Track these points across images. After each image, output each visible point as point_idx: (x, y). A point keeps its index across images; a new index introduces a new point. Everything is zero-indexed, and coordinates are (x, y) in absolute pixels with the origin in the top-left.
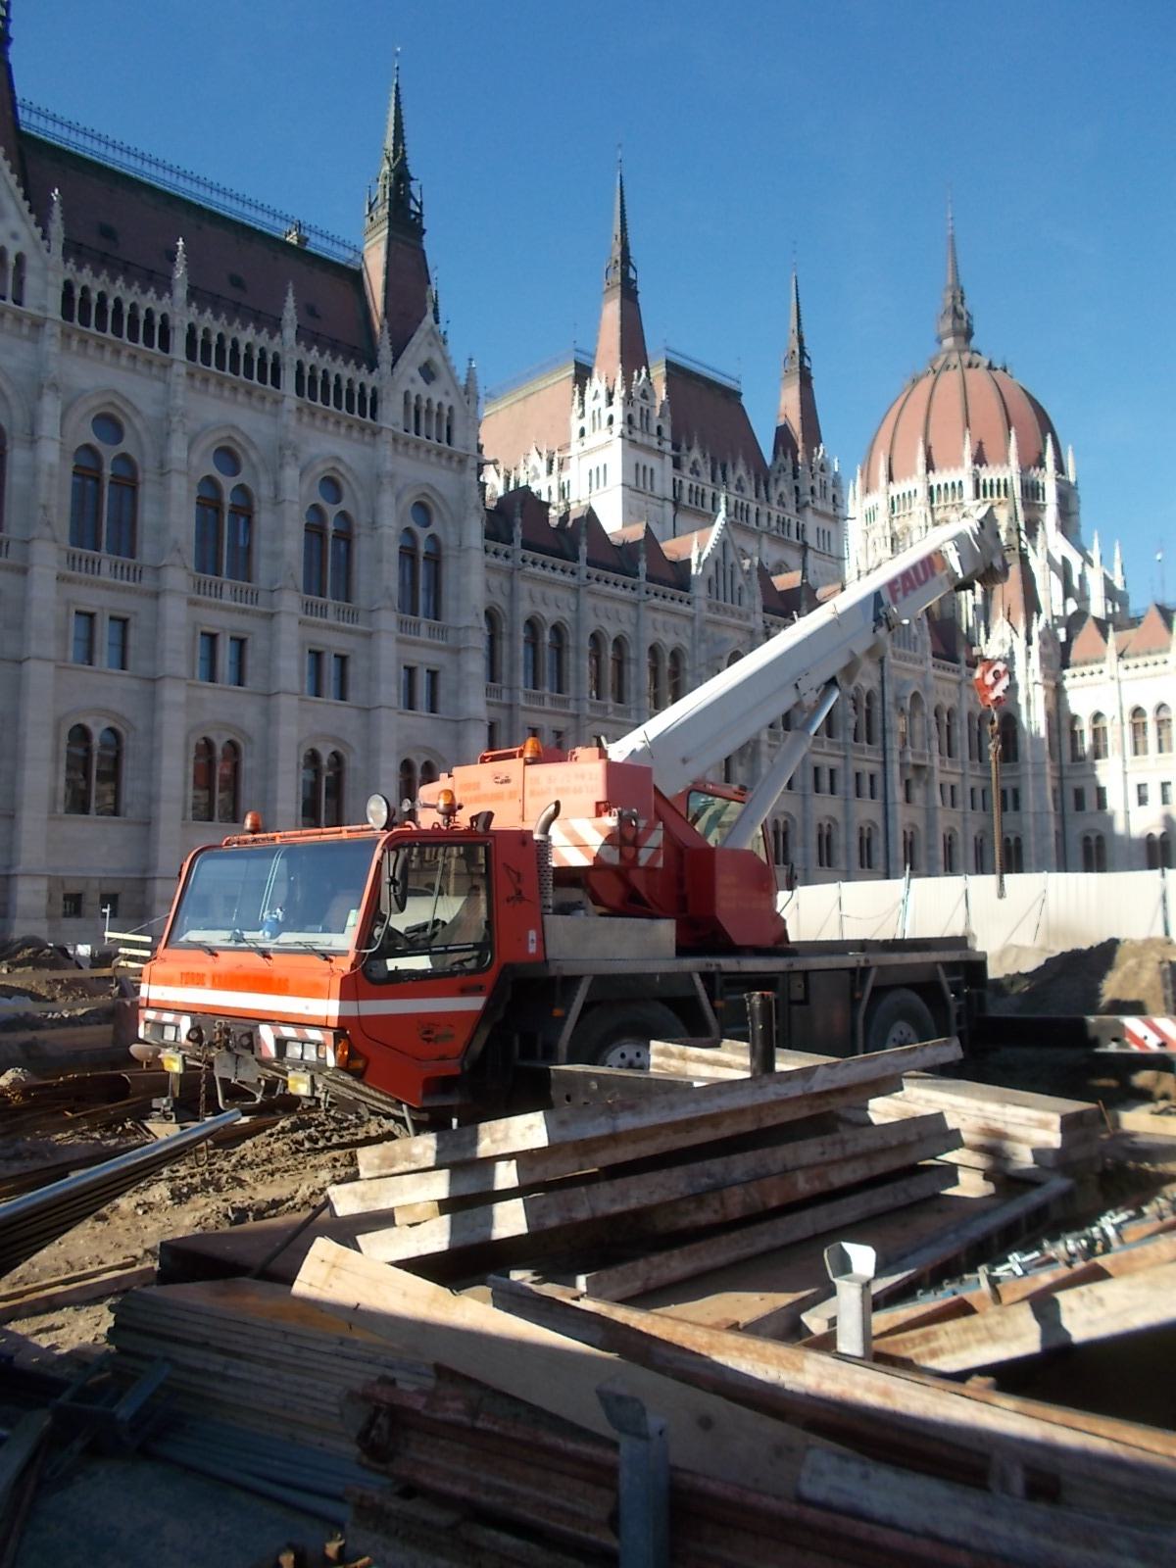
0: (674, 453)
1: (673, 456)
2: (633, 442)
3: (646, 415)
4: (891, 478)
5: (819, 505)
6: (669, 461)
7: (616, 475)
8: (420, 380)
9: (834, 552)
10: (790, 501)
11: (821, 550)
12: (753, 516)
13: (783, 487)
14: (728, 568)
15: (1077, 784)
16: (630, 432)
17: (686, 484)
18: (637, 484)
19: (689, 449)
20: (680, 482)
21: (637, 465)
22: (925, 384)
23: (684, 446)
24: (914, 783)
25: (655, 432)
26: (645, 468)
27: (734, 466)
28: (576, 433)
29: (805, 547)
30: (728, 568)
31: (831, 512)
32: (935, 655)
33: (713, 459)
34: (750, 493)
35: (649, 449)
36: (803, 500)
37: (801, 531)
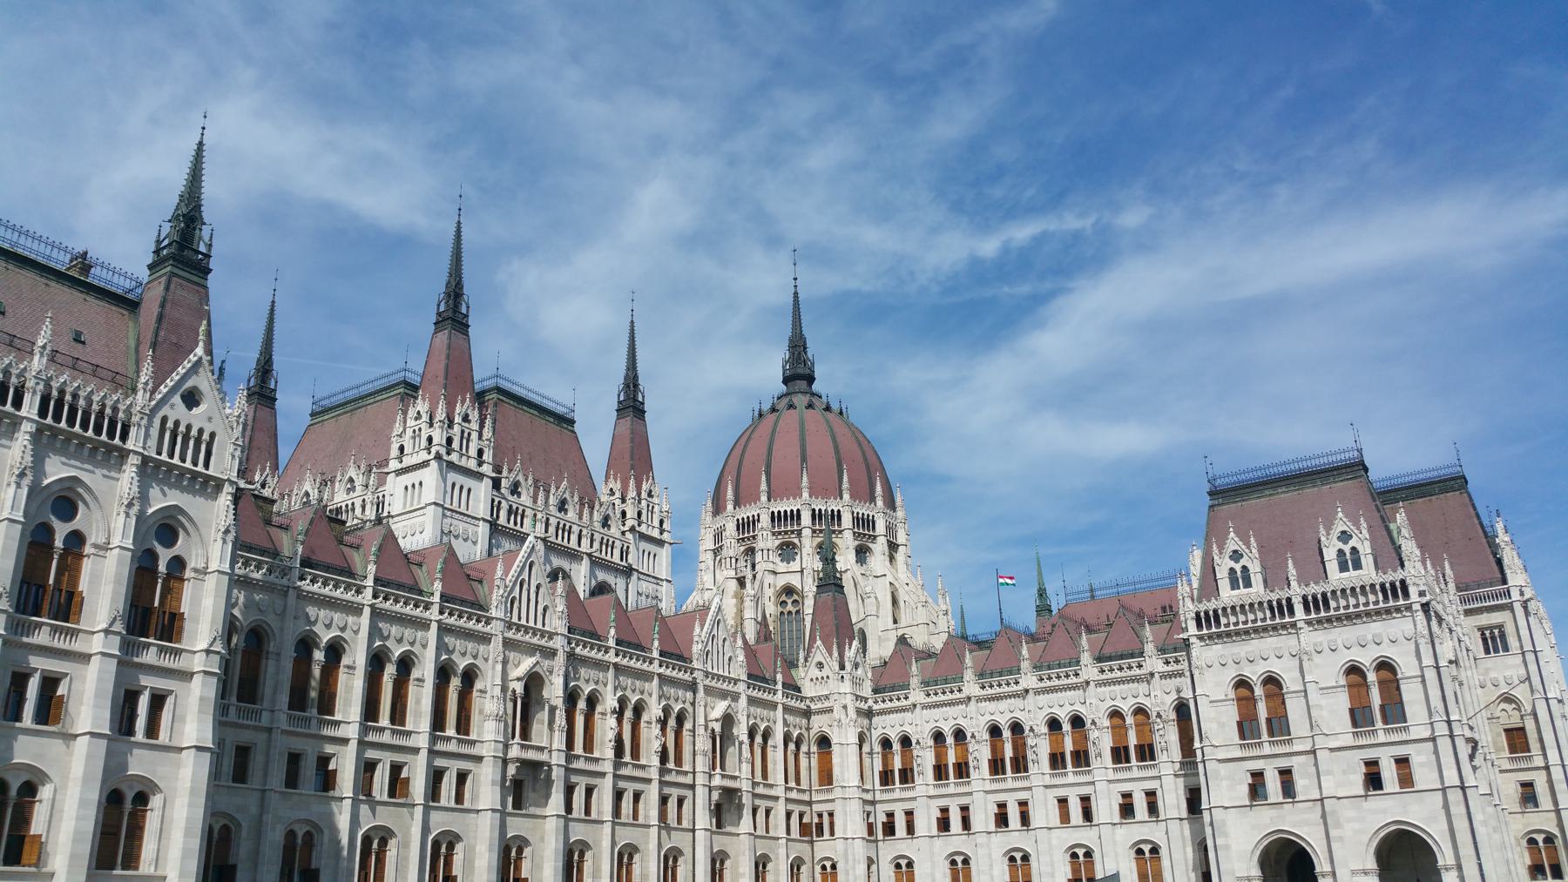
2: (452, 466)
4: (737, 503)
6: (487, 483)
7: (430, 493)
12: (574, 538)
14: (533, 589)
15: (889, 807)
16: (448, 453)
24: (725, 807)
28: (394, 452)
32: (750, 676)
37: (624, 553)
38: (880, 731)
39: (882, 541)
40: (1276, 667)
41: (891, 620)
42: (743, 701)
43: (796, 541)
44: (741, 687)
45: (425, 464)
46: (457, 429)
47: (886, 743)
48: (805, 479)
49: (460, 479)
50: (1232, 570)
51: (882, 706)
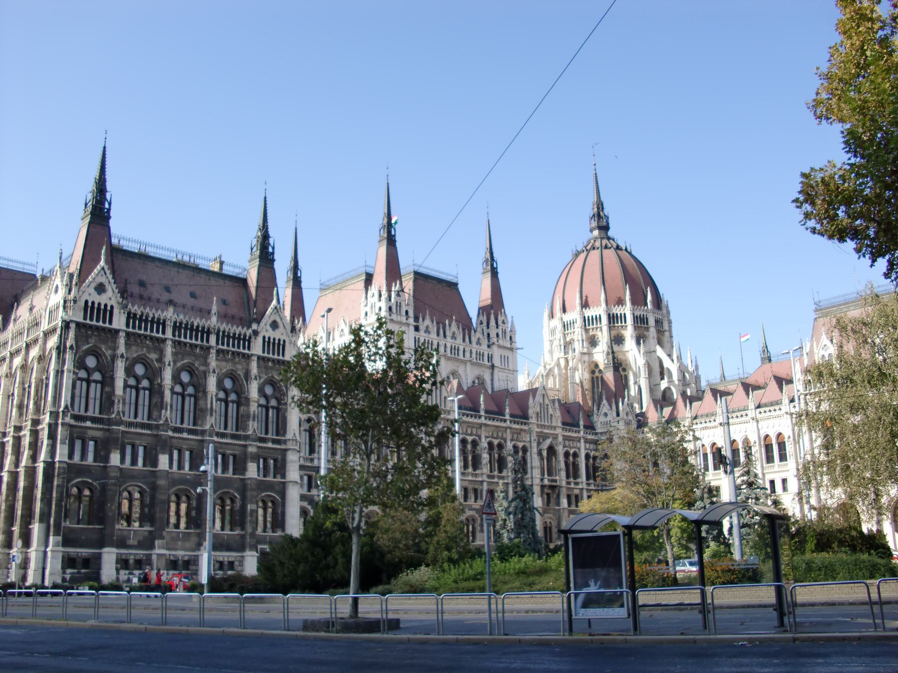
3: (399, 305)
5: (501, 342)
6: (412, 328)
8: (270, 329)
9: (511, 368)
10: (485, 342)
12: (461, 352)
13: (479, 335)
19: (423, 320)
22: (583, 256)
23: (421, 319)
25: (404, 313)
28: (363, 315)
29: (493, 367)
32: (564, 423)
33: (438, 323)
34: (459, 340)
37: (490, 358)
42: (560, 439)
44: (559, 431)
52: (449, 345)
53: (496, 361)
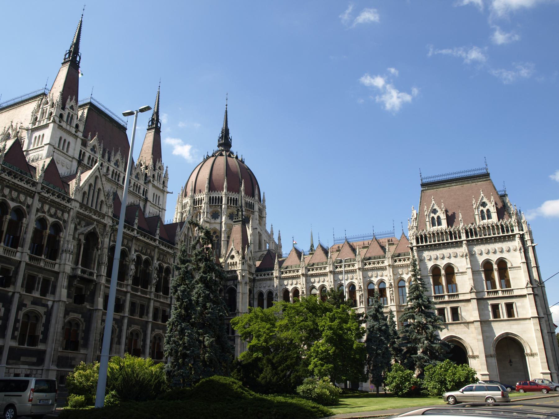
0: (83, 138)
1: (82, 140)
5: (155, 183)
6: (79, 142)
7: (47, 140)
11: (154, 203)
14: (96, 190)
16: (60, 122)
17: (87, 155)
18: (59, 147)
20: (84, 153)
21: (61, 138)
25: (74, 126)
26: (65, 141)
27: (115, 155)
29: (146, 200)
30: (96, 190)
31: (162, 188)
35: (69, 133)
36: (148, 179)
37: (145, 192)
38: (258, 289)
39: (257, 214)
40: (452, 261)
41: (258, 247)
43: (219, 210)
45: (46, 126)
46: (67, 111)
47: (261, 294)
48: (225, 184)
49: (65, 136)
50: (433, 218)
51: (259, 277)
52: (111, 169)
53: (150, 197)
